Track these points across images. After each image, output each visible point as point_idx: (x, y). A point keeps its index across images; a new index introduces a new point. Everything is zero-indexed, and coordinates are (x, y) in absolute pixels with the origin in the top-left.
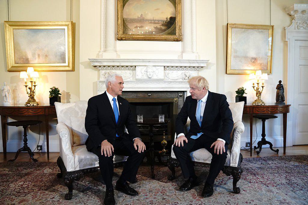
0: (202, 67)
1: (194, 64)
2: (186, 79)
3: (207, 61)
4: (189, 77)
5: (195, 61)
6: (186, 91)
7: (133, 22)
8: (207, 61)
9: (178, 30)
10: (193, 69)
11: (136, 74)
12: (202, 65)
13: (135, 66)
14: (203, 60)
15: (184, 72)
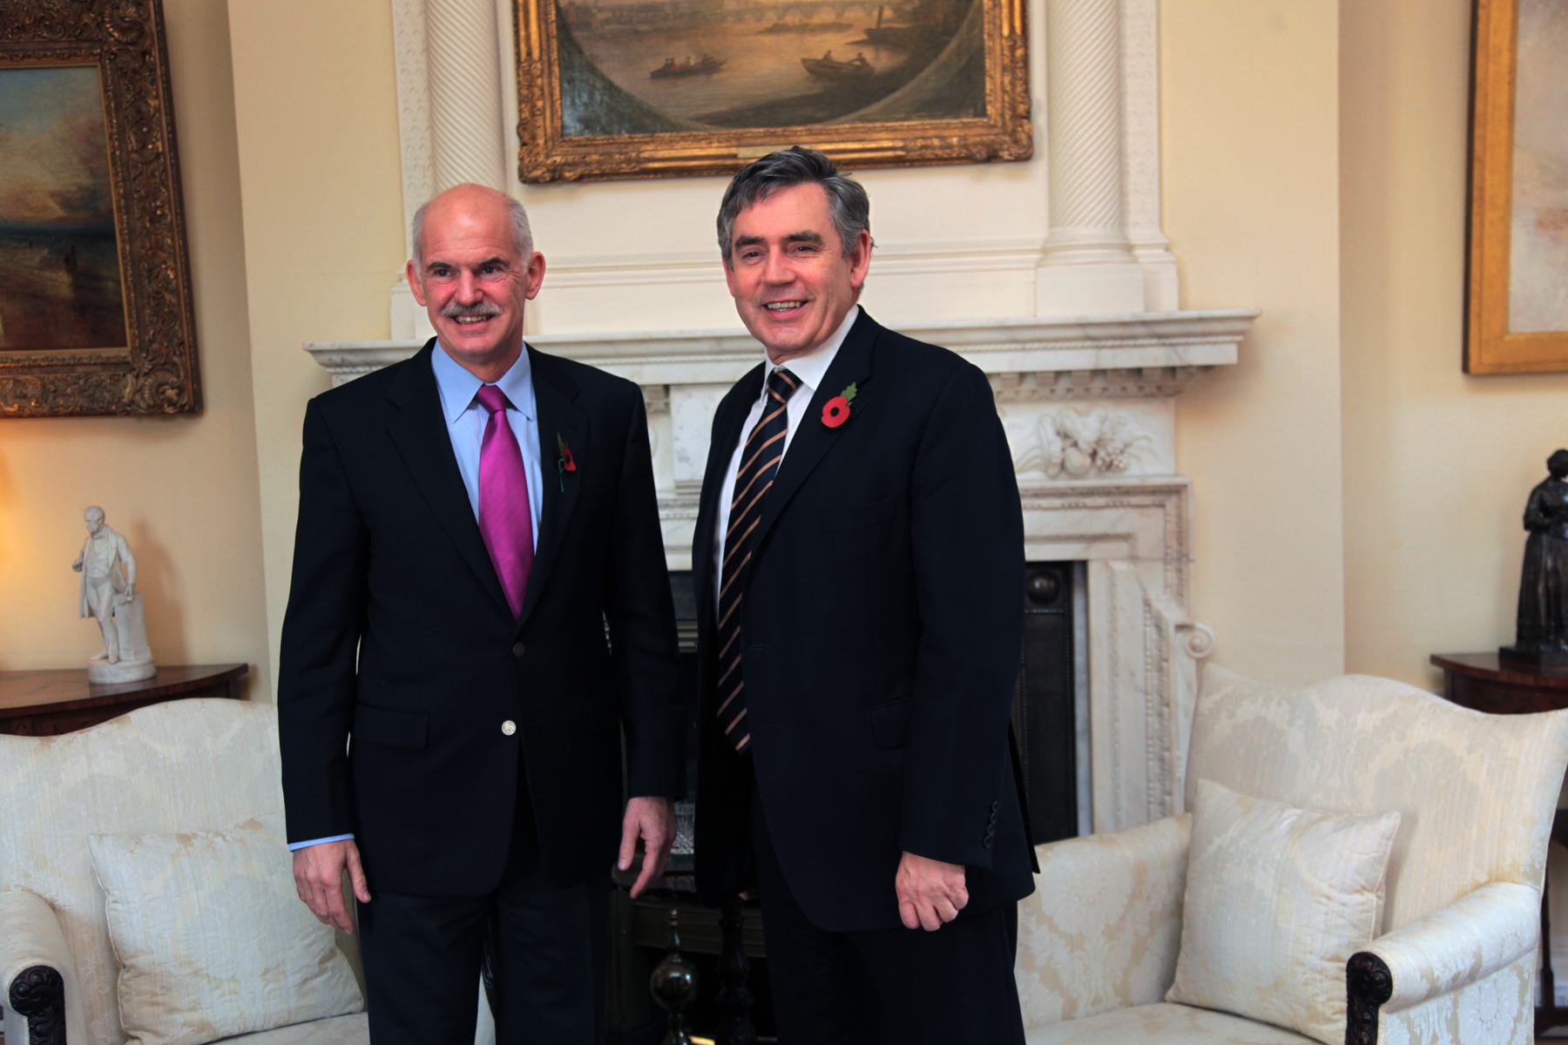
0: (1207, 369)
1: (1137, 352)
2: (1068, 465)
3: (1240, 326)
4: (1102, 454)
5: (1140, 330)
6: (1084, 564)
7: (636, 32)
8: (1240, 326)
9: (1004, 69)
10: (1131, 386)
11: (677, 445)
12: (1199, 355)
13: (667, 388)
14: (1201, 320)
15: (1052, 410)
